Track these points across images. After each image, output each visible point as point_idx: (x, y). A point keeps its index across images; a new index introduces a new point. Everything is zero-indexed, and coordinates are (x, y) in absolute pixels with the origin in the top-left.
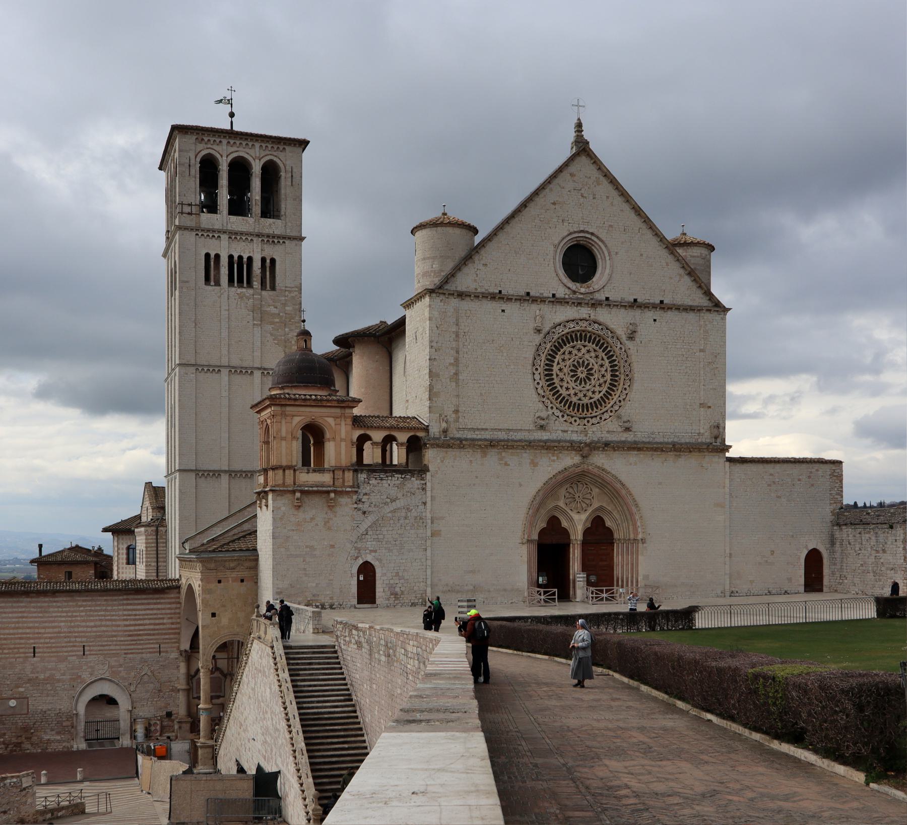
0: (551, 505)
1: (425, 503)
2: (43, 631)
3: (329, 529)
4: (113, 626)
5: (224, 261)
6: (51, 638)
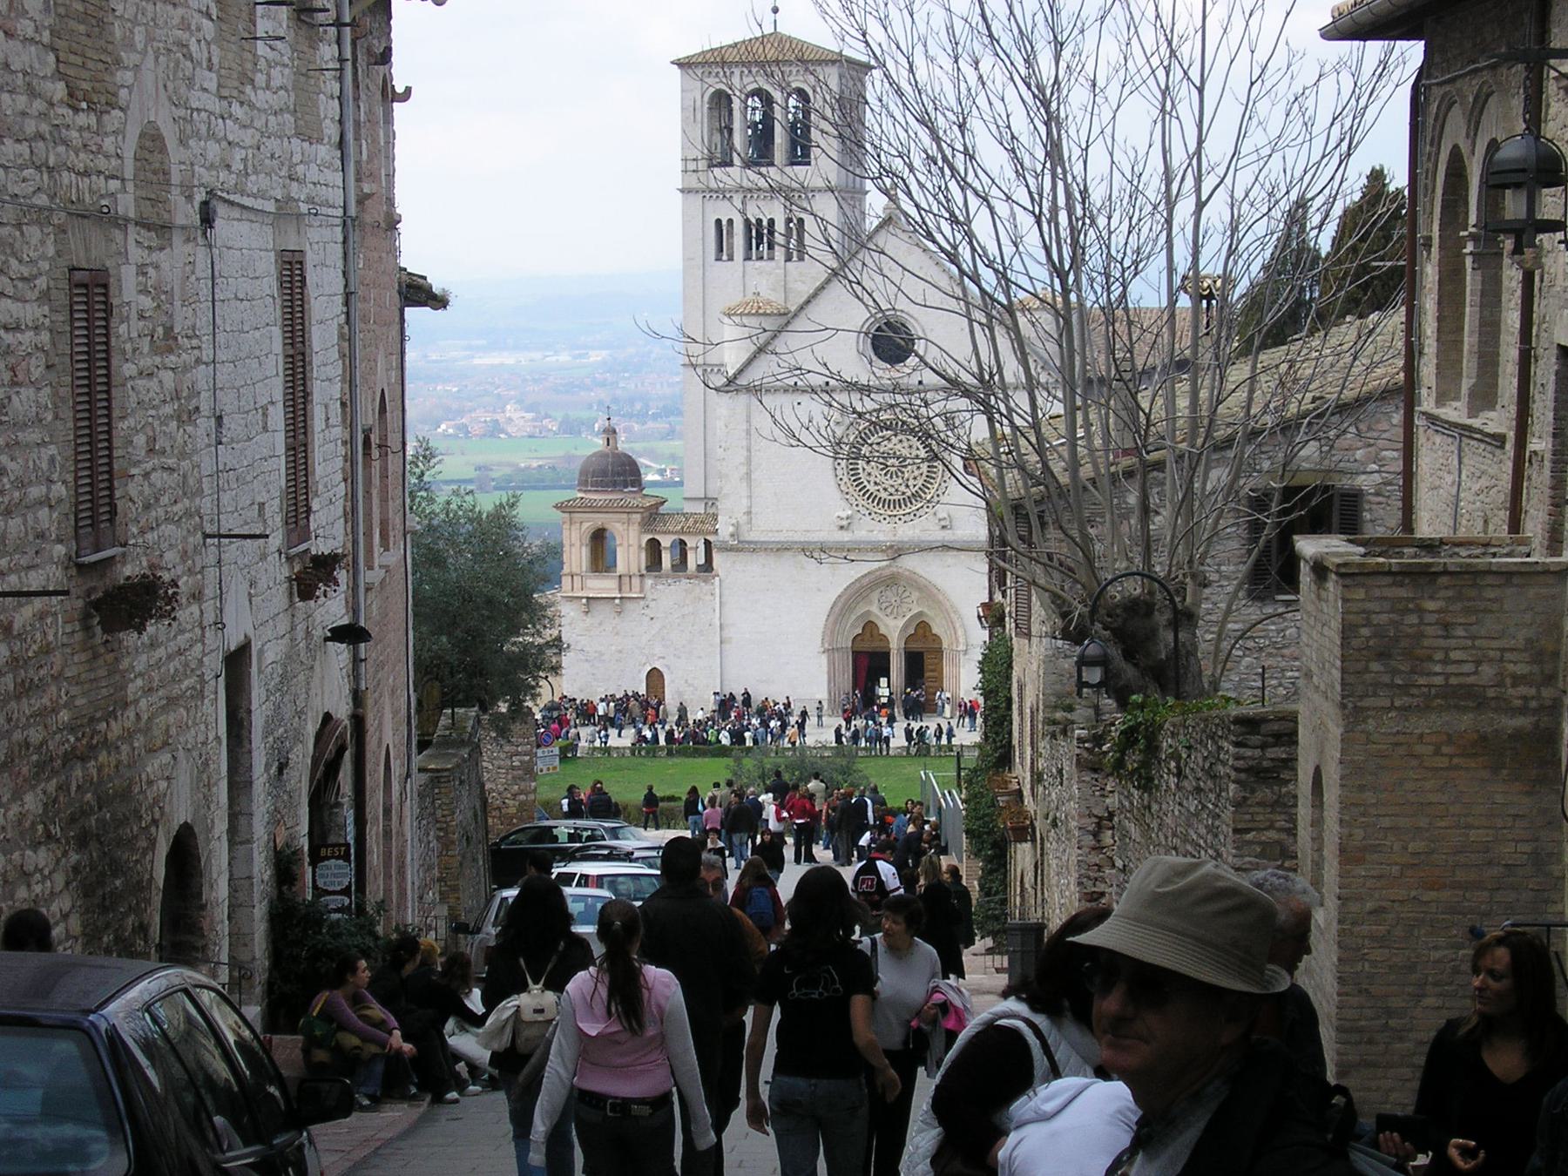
0: (861, 609)
3: (617, 634)
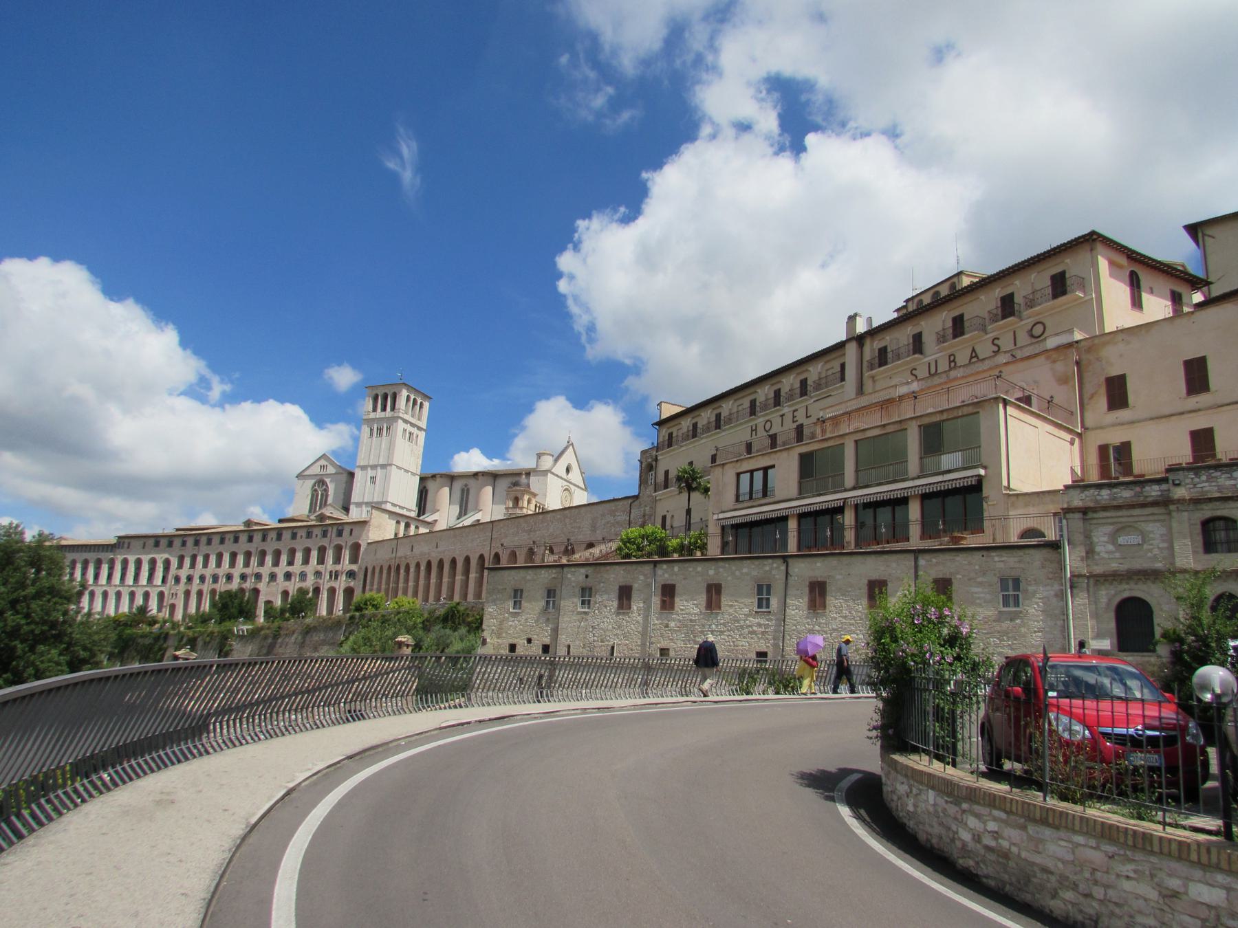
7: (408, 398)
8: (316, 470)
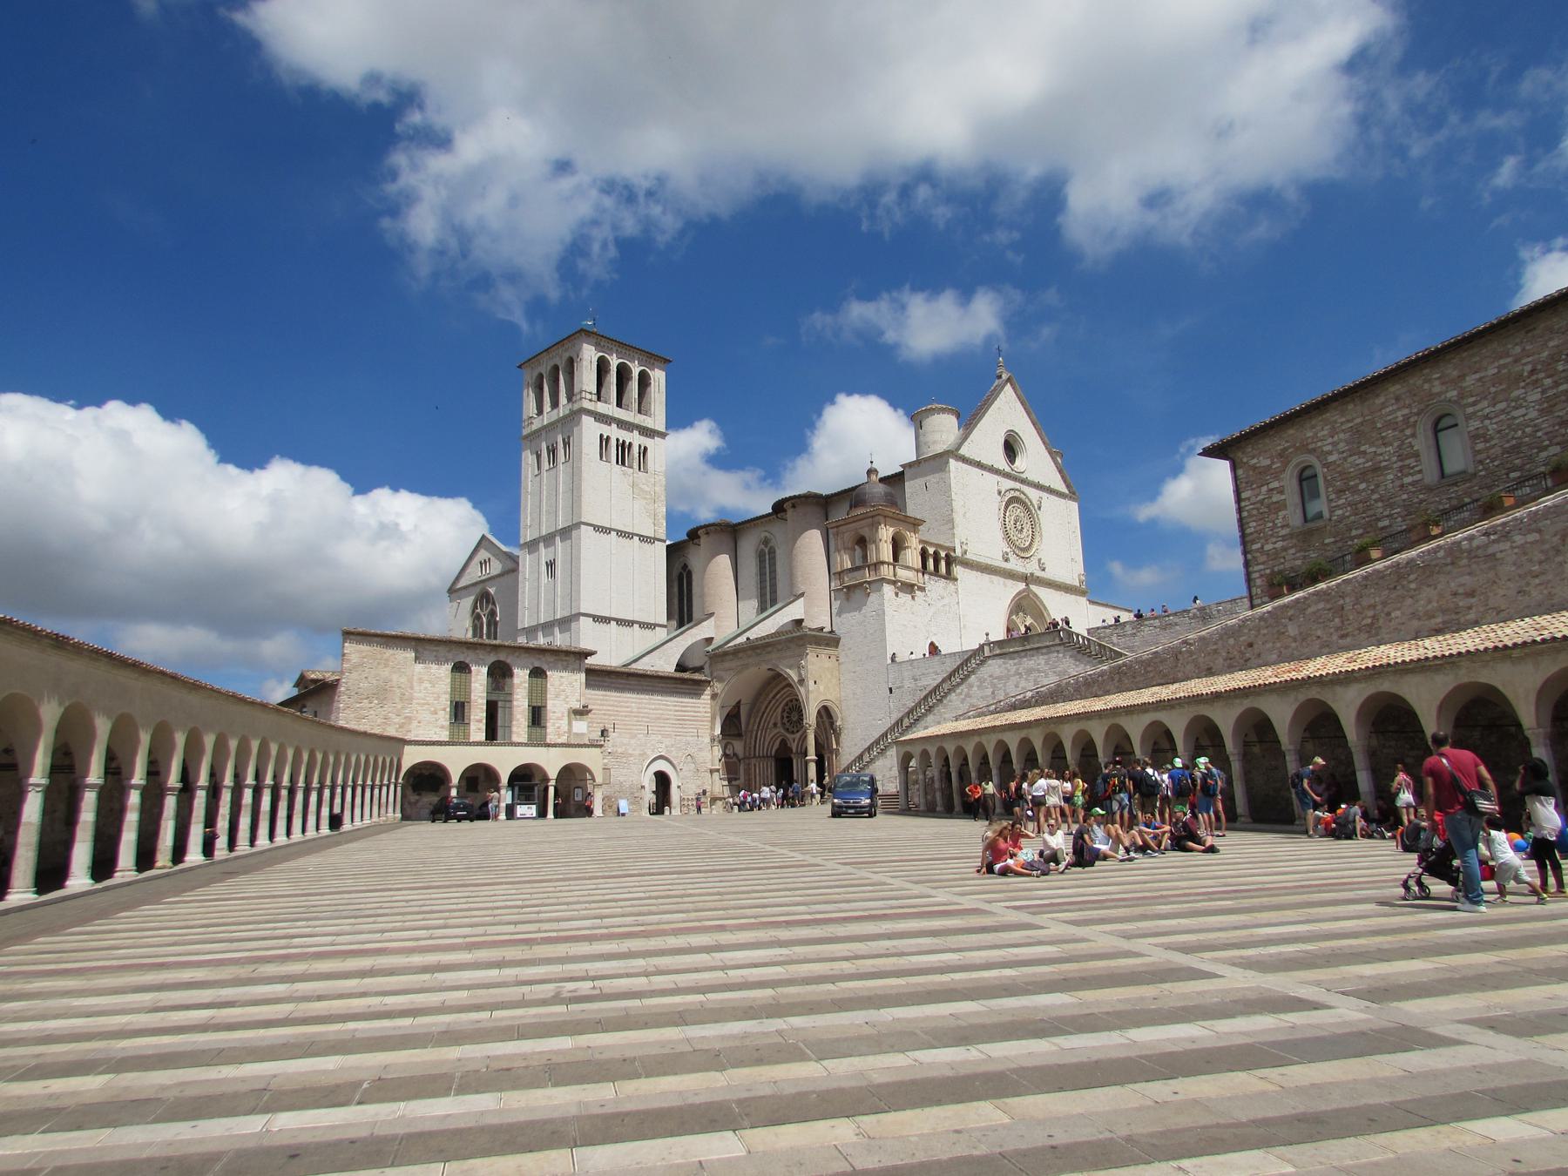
1: (958, 603)
2: (619, 709)
3: (913, 613)
4: (667, 710)
5: (613, 443)
6: (626, 716)
7: (602, 368)
8: (474, 574)
